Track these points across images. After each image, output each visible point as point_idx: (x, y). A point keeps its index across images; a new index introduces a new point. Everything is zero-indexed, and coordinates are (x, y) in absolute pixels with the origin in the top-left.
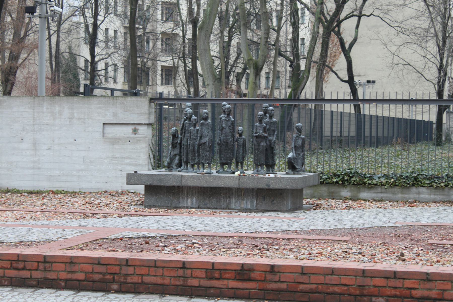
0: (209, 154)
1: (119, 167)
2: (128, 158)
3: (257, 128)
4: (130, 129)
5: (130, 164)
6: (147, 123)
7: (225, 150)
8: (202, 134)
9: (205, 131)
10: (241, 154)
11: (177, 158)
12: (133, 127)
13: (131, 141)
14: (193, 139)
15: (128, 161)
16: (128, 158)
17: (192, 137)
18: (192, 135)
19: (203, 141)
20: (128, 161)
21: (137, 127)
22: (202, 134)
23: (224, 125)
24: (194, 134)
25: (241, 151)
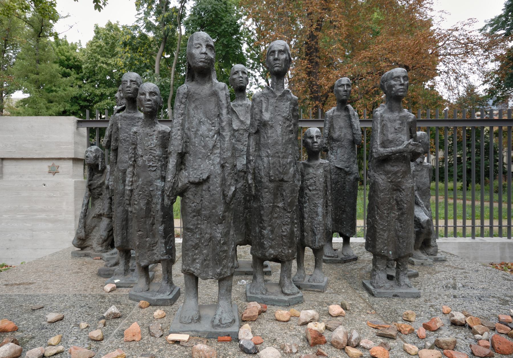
0: (226, 234)
1: (28, 225)
2: (43, 211)
3: (384, 126)
4: (45, 166)
5: (46, 220)
6: (73, 157)
7: (274, 207)
8: (186, 141)
9: (203, 129)
10: (320, 218)
11: (105, 222)
12: (50, 163)
13: (47, 185)
14: (145, 167)
15: (43, 216)
16: (43, 211)
17: (140, 161)
18: (140, 152)
19: (188, 175)
20: (43, 216)
21: (57, 163)
22: (186, 141)
23: (266, 116)
24: (149, 151)
25: (320, 210)
